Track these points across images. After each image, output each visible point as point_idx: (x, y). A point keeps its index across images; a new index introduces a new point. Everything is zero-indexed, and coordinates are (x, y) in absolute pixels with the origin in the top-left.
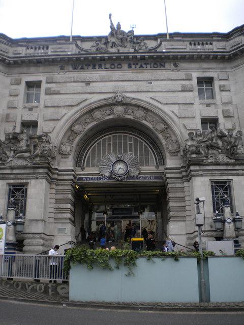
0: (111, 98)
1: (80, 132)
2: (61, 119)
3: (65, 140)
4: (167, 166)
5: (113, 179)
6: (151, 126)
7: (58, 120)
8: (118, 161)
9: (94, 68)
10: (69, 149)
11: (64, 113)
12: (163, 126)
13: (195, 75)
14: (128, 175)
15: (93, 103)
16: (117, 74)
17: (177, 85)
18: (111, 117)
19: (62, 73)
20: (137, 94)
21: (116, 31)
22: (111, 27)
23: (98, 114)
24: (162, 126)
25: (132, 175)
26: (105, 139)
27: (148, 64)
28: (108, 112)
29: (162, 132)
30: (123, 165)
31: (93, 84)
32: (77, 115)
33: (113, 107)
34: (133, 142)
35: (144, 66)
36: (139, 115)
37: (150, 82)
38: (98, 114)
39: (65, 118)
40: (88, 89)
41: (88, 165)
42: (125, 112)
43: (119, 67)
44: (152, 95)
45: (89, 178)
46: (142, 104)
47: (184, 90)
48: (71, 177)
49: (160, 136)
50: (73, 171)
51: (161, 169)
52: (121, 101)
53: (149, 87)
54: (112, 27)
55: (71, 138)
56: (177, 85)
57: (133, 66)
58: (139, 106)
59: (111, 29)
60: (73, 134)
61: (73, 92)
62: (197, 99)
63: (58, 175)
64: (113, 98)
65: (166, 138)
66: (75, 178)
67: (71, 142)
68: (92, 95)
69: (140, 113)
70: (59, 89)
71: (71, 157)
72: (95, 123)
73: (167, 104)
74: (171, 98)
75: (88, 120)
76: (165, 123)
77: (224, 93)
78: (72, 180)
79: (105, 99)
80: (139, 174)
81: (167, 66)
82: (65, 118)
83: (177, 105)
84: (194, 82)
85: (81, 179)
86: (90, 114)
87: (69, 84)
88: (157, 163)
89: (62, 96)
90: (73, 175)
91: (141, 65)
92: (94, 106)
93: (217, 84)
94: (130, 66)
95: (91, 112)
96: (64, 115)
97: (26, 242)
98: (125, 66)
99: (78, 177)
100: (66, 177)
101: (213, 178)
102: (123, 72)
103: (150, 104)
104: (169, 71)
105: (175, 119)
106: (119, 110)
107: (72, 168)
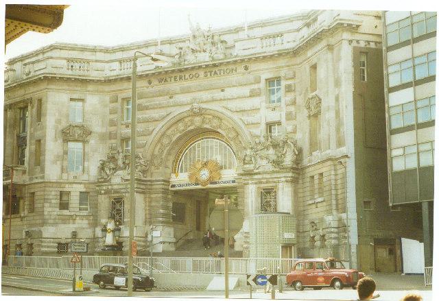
7: (149, 135)
11: (151, 129)
13: (265, 76)
17: (246, 91)
18: (192, 128)
29: (234, 139)
32: (163, 130)
35: (218, 72)
41: (181, 172)
42: (203, 122)
44: (224, 104)
46: (216, 114)
47: (253, 94)
53: (221, 95)
56: (246, 91)
62: (264, 104)
63: (151, 185)
69: (215, 122)
72: (179, 134)
77: (289, 94)
82: (155, 133)
84: (262, 85)
85: (173, 186)
93: (284, 83)
97: (124, 244)
98: (202, 73)
100: (157, 187)
101: (262, 185)
105: (243, 127)
106: (198, 121)
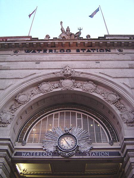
0: (60, 72)
1: (25, 102)
2: (6, 89)
3: (8, 109)
4: (125, 137)
5: (59, 155)
6: (102, 98)
8: (65, 134)
9: (45, 51)
10: (9, 117)
11: (9, 84)
12: (116, 98)
14: (76, 149)
15: (40, 76)
16: (66, 56)
19: (15, 55)
20: (86, 69)
21: (66, 32)
22: (61, 29)
23: (45, 87)
24: (113, 97)
25: (82, 150)
26: (53, 114)
27: (95, 50)
28: (56, 85)
29: (114, 103)
30: (71, 139)
31: (41, 63)
33: (61, 81)
34: (82, 119)
36: (88, 88)
37: (97, 61)
38: (45, 87)
39: (10, 88)
40: (38, 66)
43: (69, 51)
44: (101, 70)
45: (29, 153)
48: (6, 147)
49: (113, 106)
50: (9, 140)
51: (116, 145)
52: (70, 75)
53: (98, 65)
54: (62, 30)
55: (14, 107)
57: (81, 51)
58: (88, 80)
59: (62, 31)
60: (17, 104)
61: (23, 68)
64: (62, 72)
65: (120, 109)
66: (12, 152)
67: (13, 111)
68: (40, 71)
69: (88, 87)
70: (9, 66)
71: (9, 126)
72: (42, 94)
73: (117, 78)
74: (119, 73)
75: (34, 92)
76: (118, 94)
78: (7, 151)
79: (54, 73)
80: (90, 149)
81: (112, 51)
82: (10, 88)
83: (127, 79)
85: (20, 154)
86: (37, 87)
87: (18, 63)
88: (110, 139)
89: (11, 71)
90: (9, 145)
91: (89, 50)
92: (42, 79)
94: (78, 51)
95: (37, 85)
96: (10, 86)
99: (16, 151)
102: (71, 54)
103: (100, 77)
104: (115, 54)
107: (9, 137)
